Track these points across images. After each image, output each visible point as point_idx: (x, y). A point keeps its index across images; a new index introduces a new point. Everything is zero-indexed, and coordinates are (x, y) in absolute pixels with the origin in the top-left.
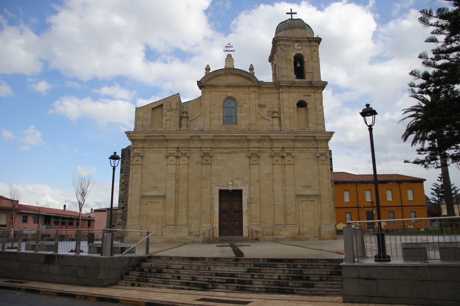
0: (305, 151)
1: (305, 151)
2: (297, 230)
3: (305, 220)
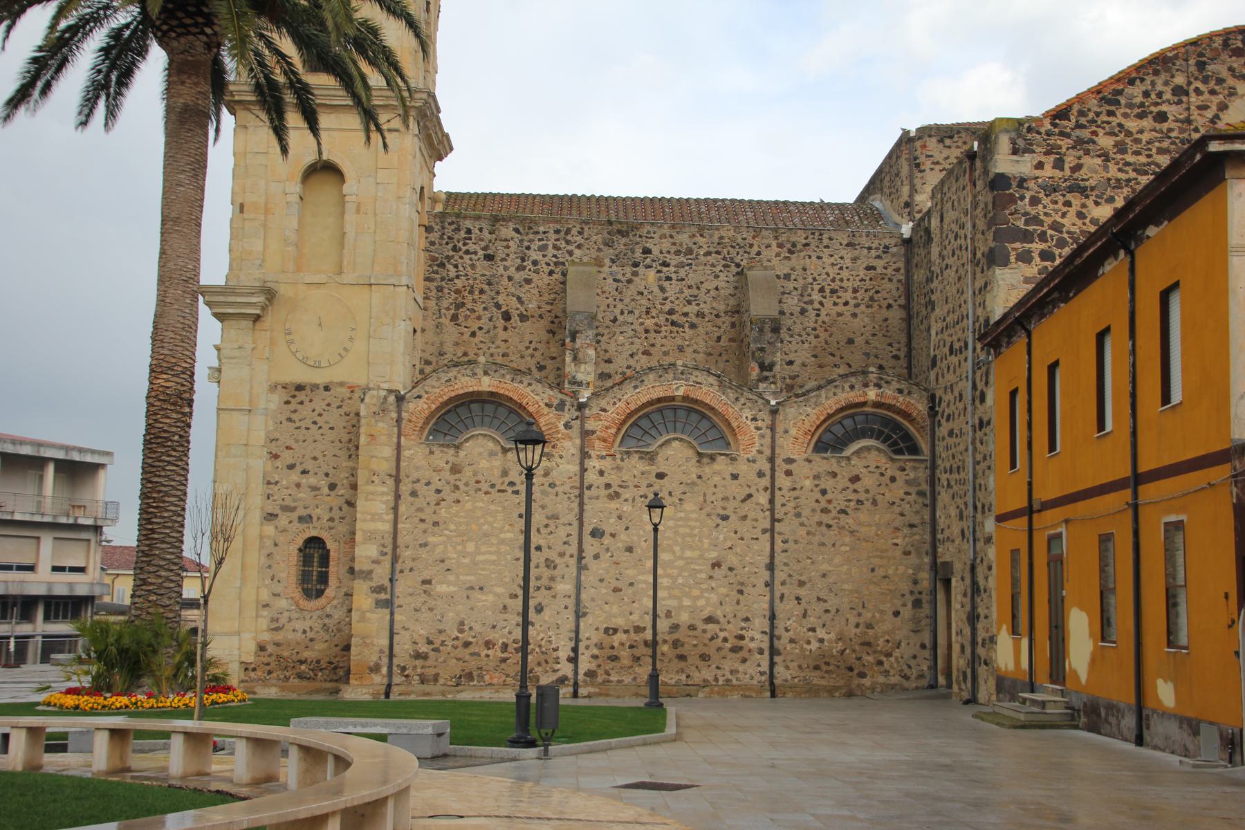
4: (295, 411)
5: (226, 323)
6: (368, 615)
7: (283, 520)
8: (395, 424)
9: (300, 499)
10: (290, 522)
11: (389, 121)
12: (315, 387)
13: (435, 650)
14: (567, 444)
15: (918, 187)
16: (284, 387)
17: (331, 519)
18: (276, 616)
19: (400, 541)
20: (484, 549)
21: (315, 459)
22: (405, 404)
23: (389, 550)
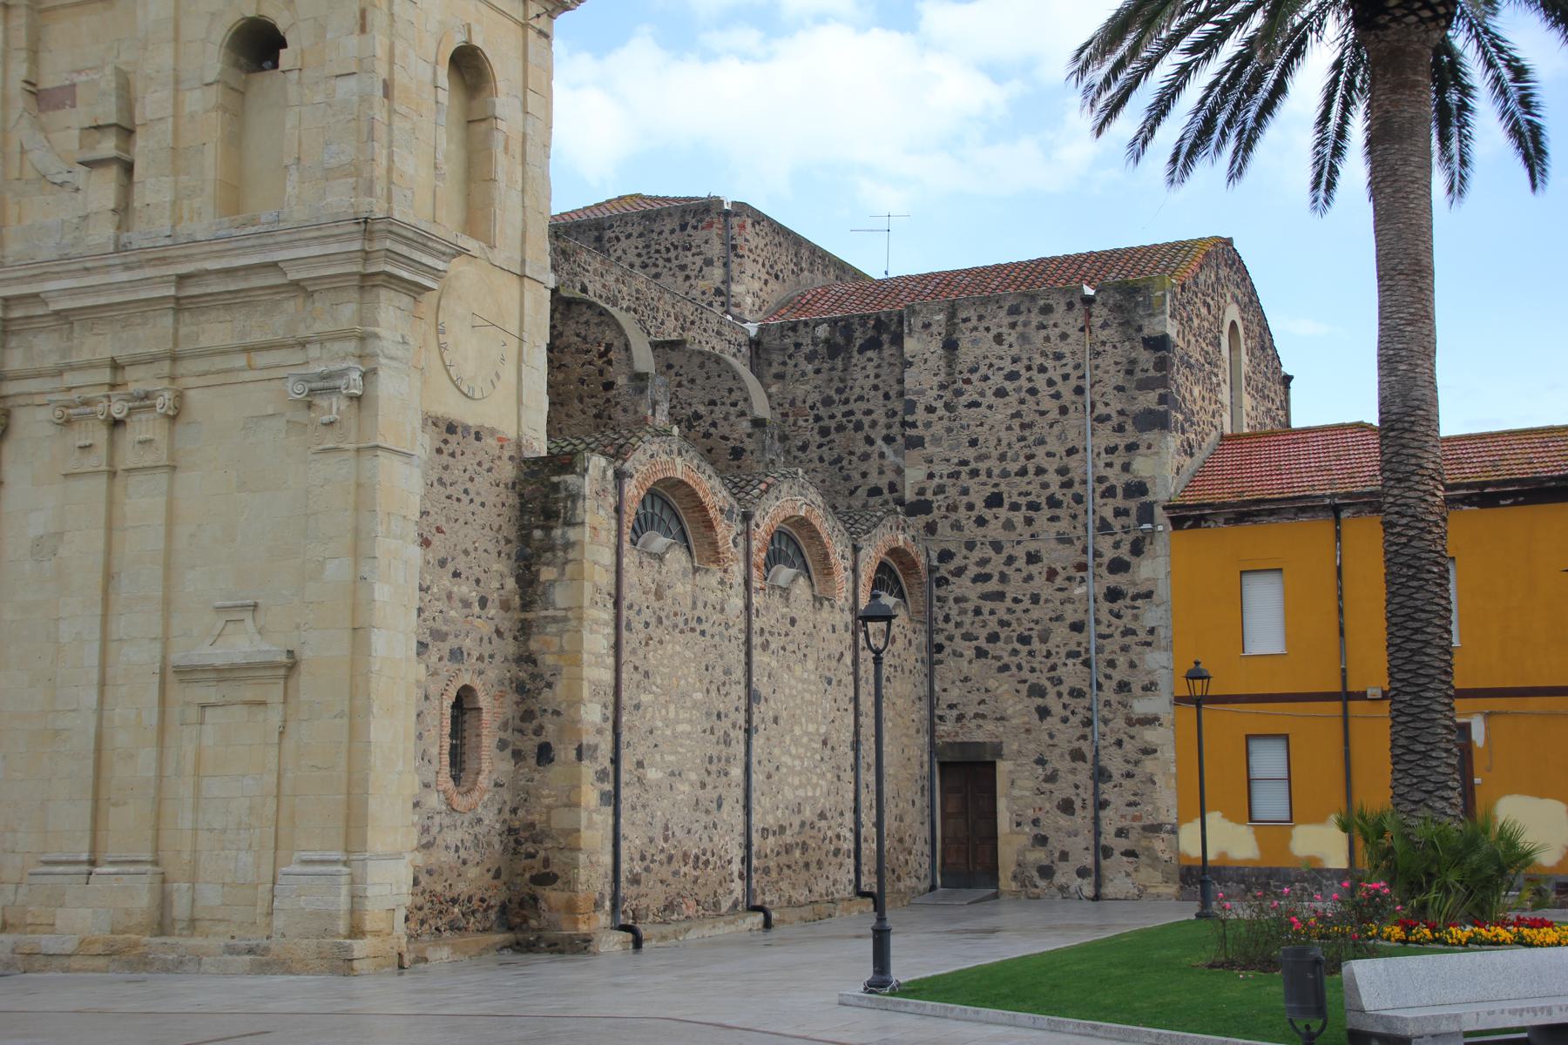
0: (241, 370)
1: (241, 370)
2: (142, 900)
3: (211, 830)
4: (446, 468)
6: (595, 816)
8: (613, 514)
9: (453, 621)
10: (441, 659)
12: (466, 428)
13: (647, 869)
15: (735, 274)
16: (435, 424)
17: (480, 658)
19: (624, 695)
20: (683, 715)
21: (466, 552)
23: (610, 712)
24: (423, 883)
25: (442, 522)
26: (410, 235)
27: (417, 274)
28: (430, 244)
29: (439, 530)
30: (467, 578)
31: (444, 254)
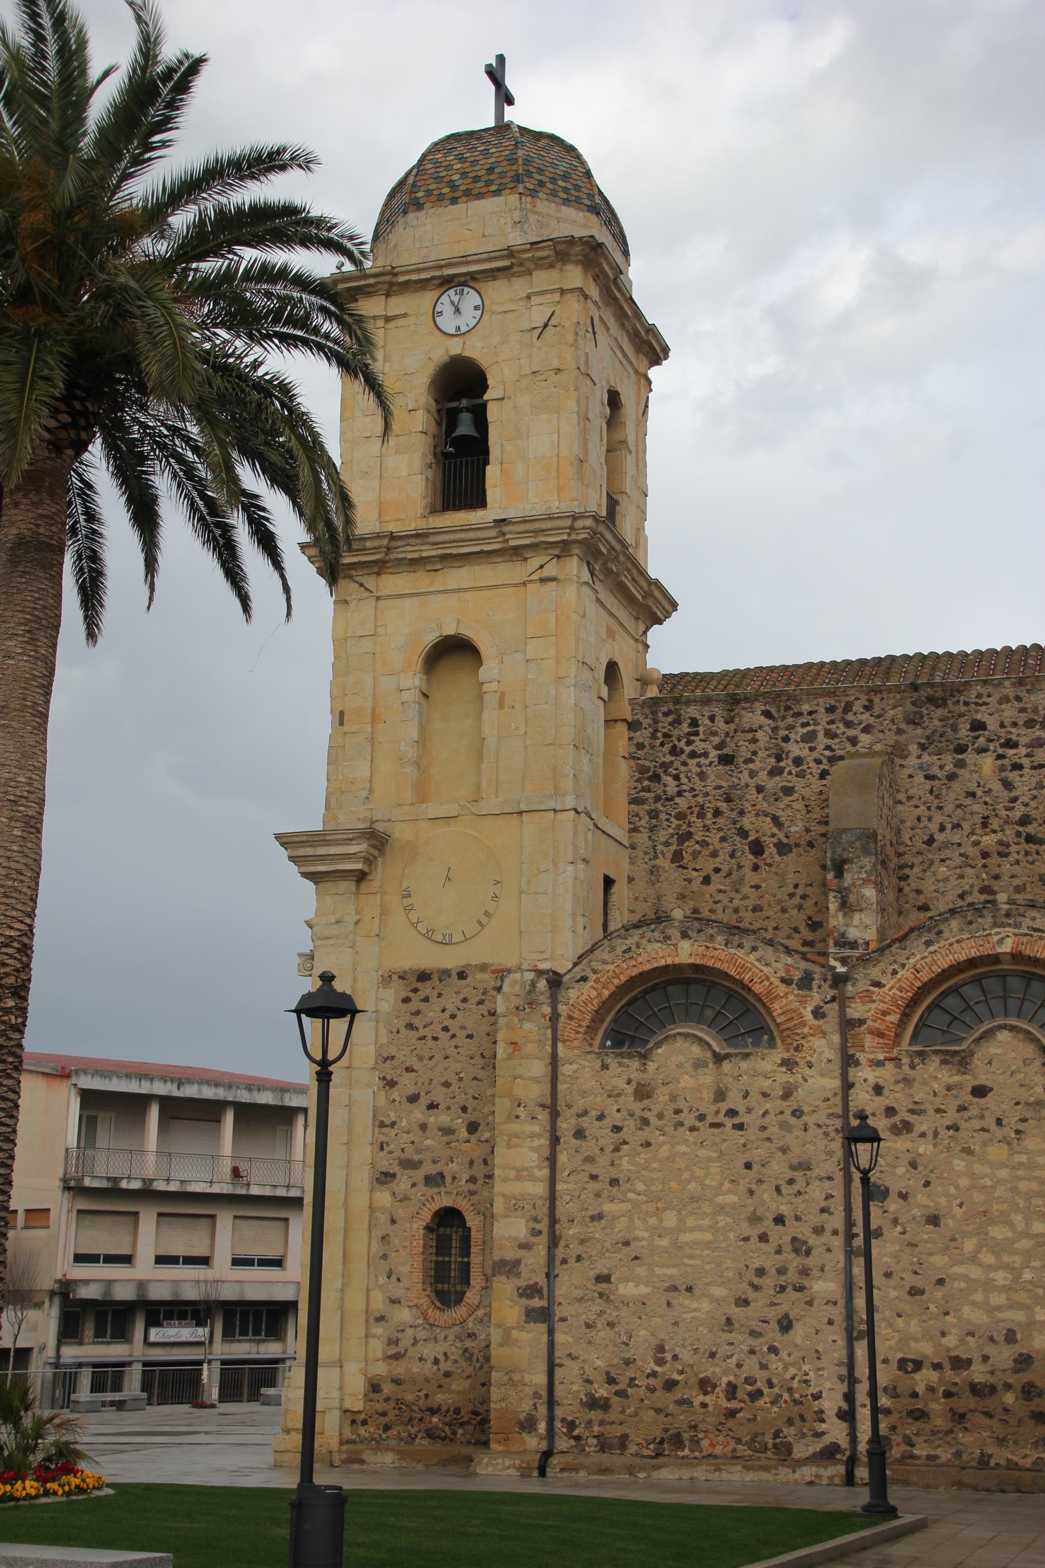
4: (417, 1013)
5: (320, 885)
6: (515, 1333)
7: (403, 1184)
9: (428, 1149)
10: (414, 1185)
11: (542, 567)
12: (445, 974)
13: (622, 1394)
14: (818, 1043)
16: (402, 978)
17: (472, 1180)
18: (394, 1335)
20: (691, 1222)
21: (447, 1084)
22: (563, 992)
23: (543, 1226)
24: (386, 1391)
25: (412, 1061)
26: (304, 839)
27: (336, 864)
28: (328, 838)
29: (409, 1070)
30: (449, 1108)
31: (351, 840)
